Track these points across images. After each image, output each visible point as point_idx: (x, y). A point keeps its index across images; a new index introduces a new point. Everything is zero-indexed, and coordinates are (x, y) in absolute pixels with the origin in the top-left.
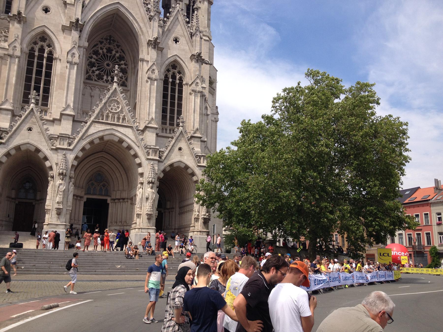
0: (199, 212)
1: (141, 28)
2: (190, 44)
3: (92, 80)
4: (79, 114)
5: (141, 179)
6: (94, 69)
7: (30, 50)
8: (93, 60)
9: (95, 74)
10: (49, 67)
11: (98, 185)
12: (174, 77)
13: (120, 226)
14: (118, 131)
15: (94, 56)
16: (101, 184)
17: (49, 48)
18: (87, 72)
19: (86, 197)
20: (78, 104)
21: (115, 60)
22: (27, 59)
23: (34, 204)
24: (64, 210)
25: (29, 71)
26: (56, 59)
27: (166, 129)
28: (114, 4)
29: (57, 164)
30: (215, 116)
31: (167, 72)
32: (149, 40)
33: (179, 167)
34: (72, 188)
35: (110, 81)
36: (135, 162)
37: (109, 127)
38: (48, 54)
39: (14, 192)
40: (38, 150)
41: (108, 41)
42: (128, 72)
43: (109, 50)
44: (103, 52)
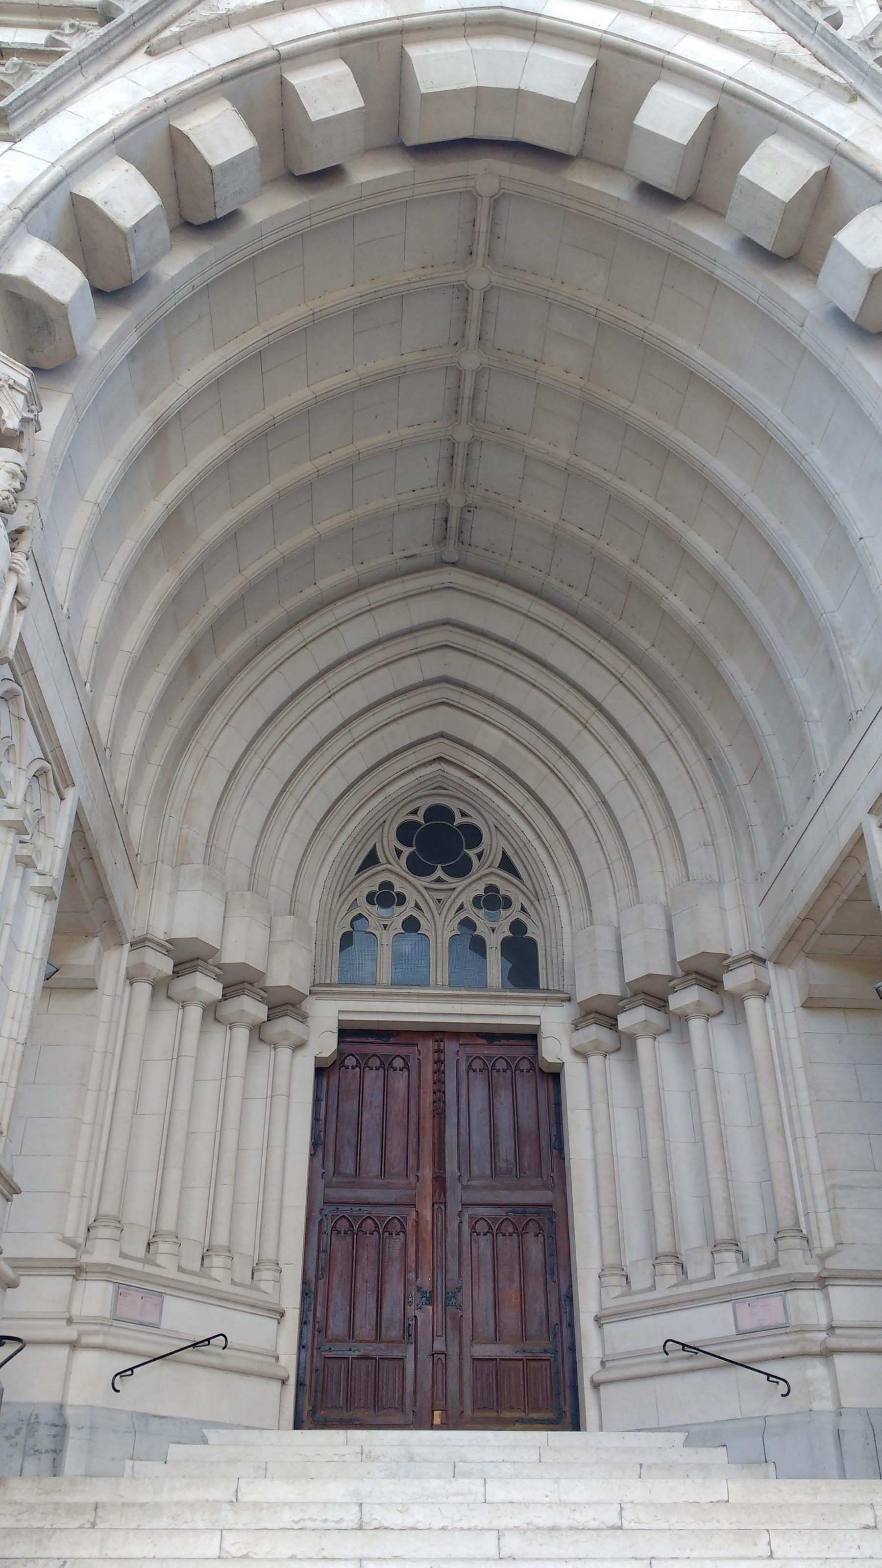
13: (726, 1295)
19: (325, 1017)
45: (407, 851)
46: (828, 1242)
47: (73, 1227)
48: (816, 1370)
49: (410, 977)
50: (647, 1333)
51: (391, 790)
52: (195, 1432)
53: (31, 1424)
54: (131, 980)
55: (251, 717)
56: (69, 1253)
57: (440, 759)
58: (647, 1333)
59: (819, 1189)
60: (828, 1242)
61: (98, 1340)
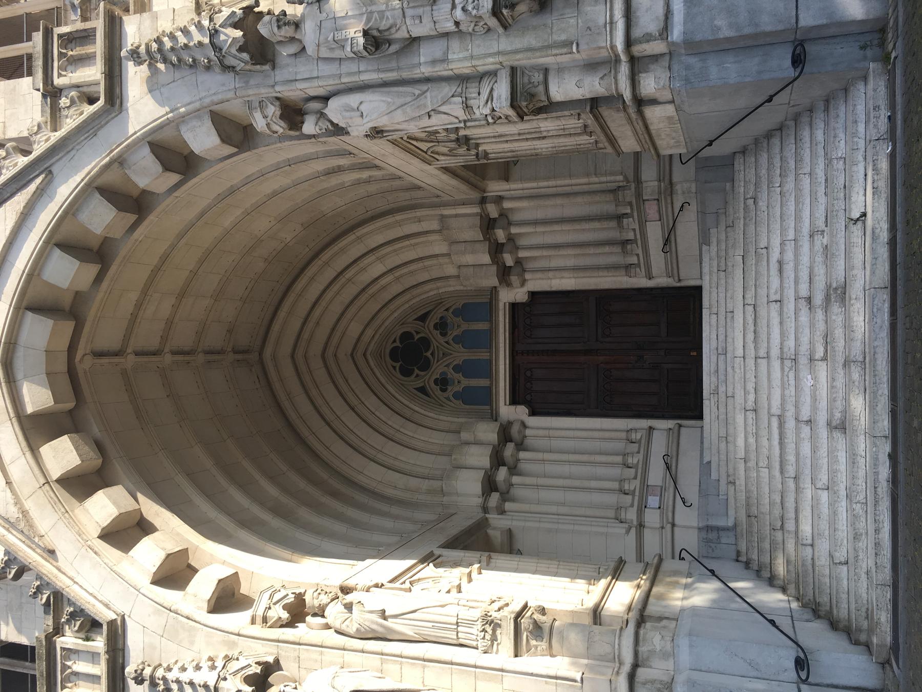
19: (507, 411)
45: (416, 371)
46: (621, 178)
47: (620, 529)
48: (678, 188)
49: (487, 369)
50: (657, 260)
51: (383, 381)
52: (706, 467)
53: (708, 541)
54: (502, 512)
55: (357, 460)
56: (633, 531)
57: (365, 355)
58: (657, 260)
59: (596, 180)
60: (621, 178)
61: (670, 515)
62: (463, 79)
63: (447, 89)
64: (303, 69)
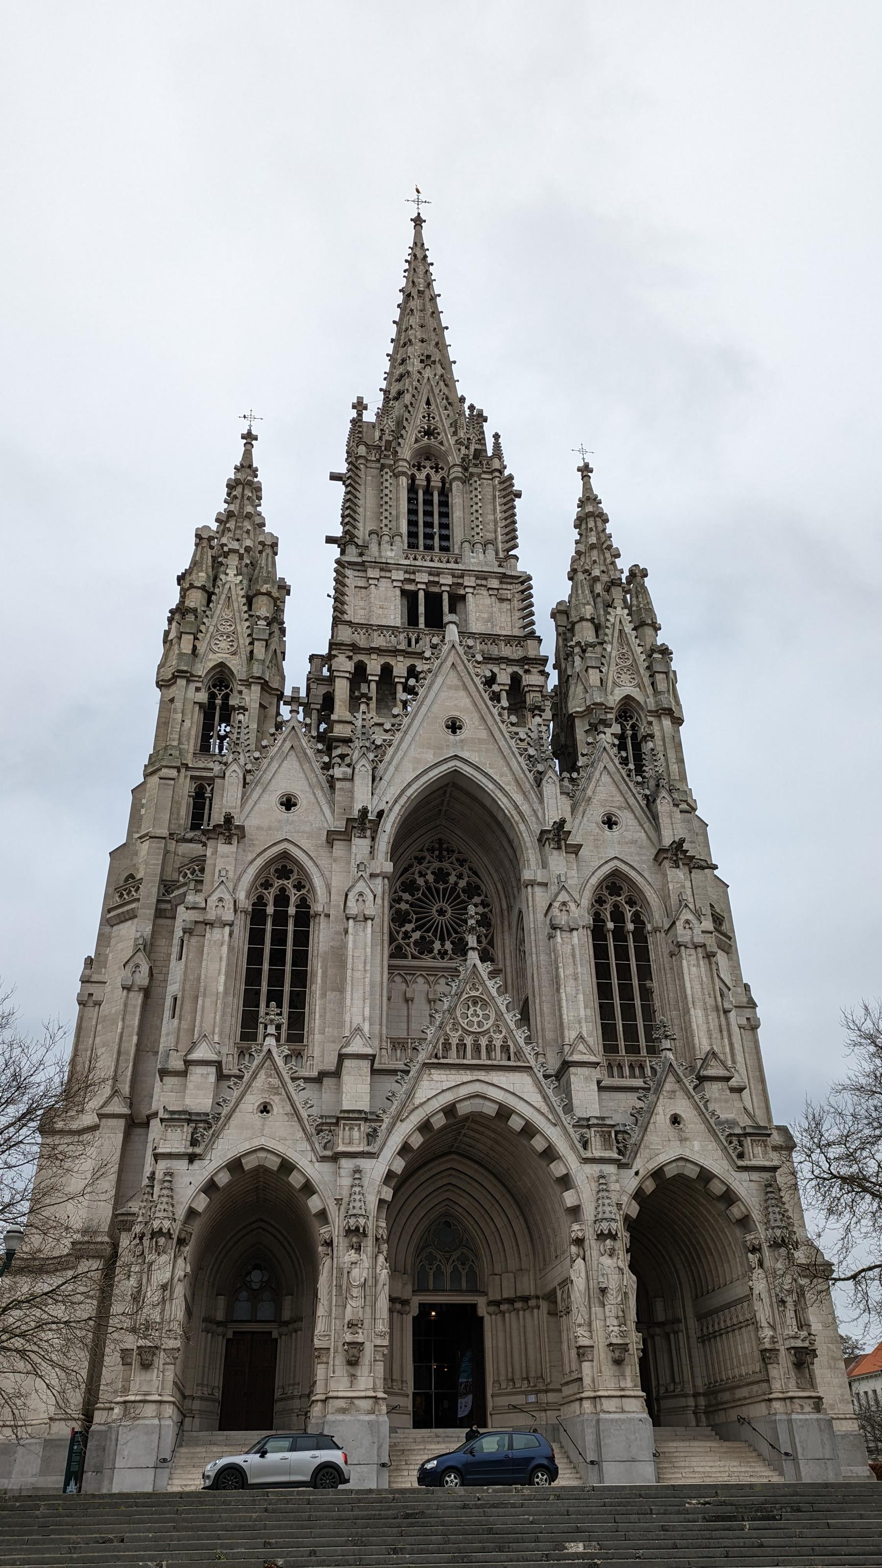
0: (773, 1327)
1: (517, 807)
2: (647, 825)
3: (405, 957)
4: (384, 1052)
5: (576, 1227)
6: (409, 927)
7: (253, 905)
8: (404, 906)
9: (412, 940)
10: (302, 939)
11: (448, 1260)
12: (618, 916)
14: (493, 1085)
15: (406, 896)
16: (456, 1255)
17: (299, 891)
18: (392, 939)
19: (416, 1301)
20: (381, 1025)
21: (458, 896)
22: (249, 926)
23: (275, 1335)
24: (368, 1348)
25: (254, 956)
26: (317, 915)
27: (620, 1067)
28: (446, 761)
29: (339, 1201)
30: (748, 1013)
31: (597, 906)
32: (543, 832)
33: (680, 1178)
34: (384, 1274)
35: (450, 952)
36: (550, 1174)
37: (467, 1076)
38: (297, 907)
39: (221, 1301)
40: (287, 1166)
41: (437, 853)
42: (493, 922)
43: (441, 875)
44: (426, 882)
48: (543, 1414)
62: (590, 1324)
63: (586, 1317)
64: (595, 1253)
